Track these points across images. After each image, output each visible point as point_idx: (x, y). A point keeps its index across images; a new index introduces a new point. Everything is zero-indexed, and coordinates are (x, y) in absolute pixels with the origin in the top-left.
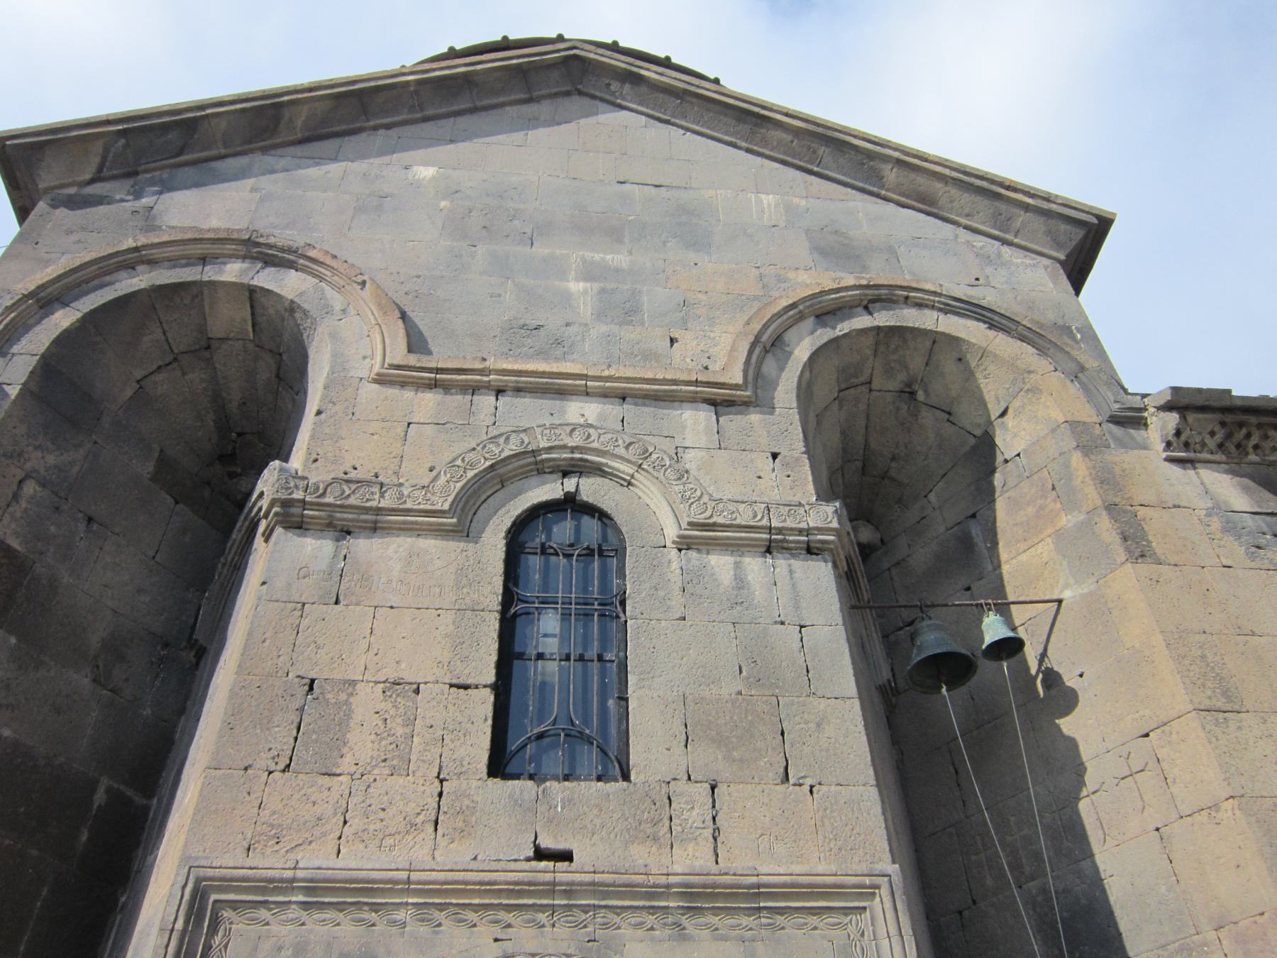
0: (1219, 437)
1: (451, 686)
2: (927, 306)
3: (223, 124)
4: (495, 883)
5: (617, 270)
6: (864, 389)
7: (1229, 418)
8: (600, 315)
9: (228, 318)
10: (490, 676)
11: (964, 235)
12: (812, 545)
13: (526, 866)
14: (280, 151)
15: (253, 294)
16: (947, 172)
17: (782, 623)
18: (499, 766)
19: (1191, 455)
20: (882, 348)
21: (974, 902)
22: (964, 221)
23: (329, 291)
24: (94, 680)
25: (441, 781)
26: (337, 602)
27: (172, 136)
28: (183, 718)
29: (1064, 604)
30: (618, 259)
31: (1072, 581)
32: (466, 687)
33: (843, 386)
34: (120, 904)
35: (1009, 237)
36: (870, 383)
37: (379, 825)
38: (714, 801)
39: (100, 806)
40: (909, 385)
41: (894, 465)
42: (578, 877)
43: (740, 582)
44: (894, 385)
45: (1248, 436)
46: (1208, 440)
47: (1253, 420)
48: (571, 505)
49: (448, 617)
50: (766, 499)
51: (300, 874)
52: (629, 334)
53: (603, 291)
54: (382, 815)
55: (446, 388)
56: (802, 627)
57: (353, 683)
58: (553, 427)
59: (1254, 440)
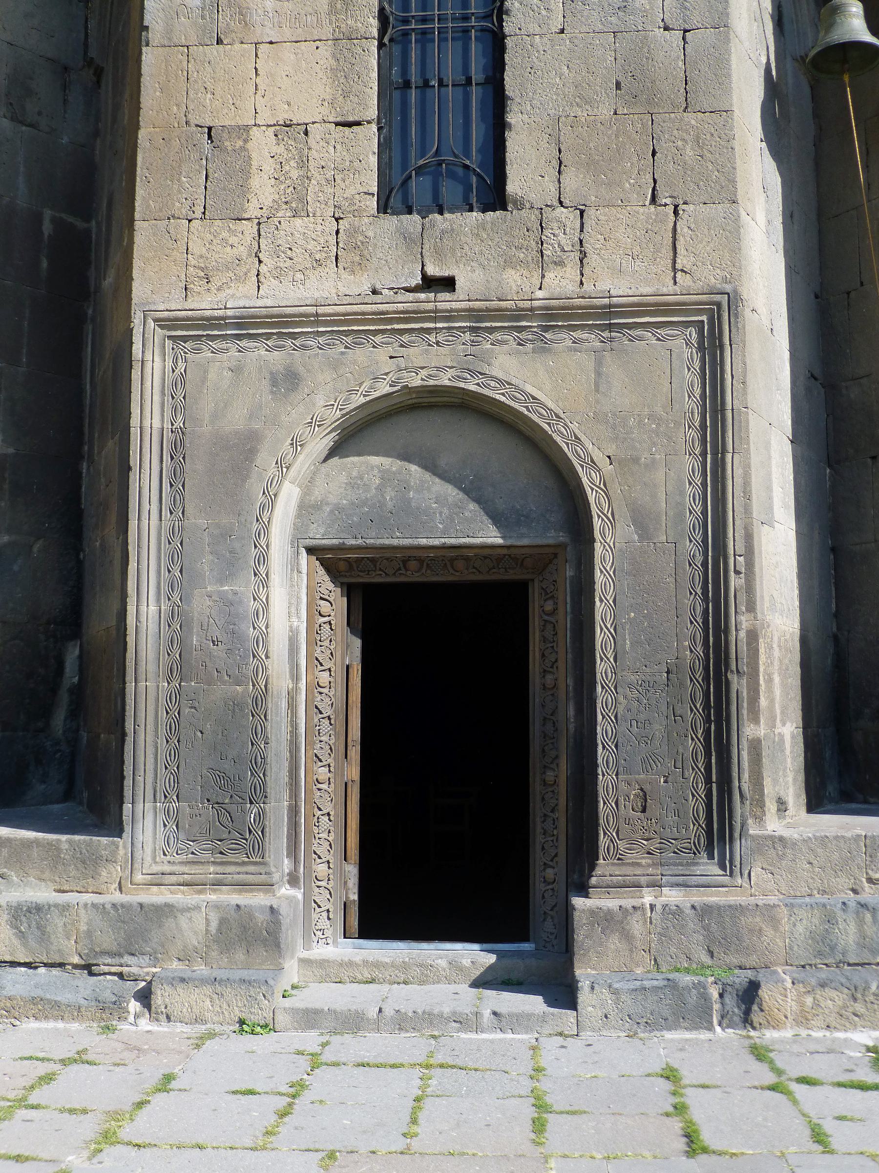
1: (337, 124)
4: (387, 313)
13: (411, 296)
17: (666, 28)
21: (862, 284)
24: (12, 119)
25: (337, 220)
26: (217, 44)
28: (98, 141)
32: (349, 125)
34: (89, 316)
37: (289, 263)
38: (582, 225)
39: (50, 236)
42: (455, 305)
49: (326, 51)
51: (230, 313)
54: (289, 252)
56: (686, 31)
57: (247, 128)
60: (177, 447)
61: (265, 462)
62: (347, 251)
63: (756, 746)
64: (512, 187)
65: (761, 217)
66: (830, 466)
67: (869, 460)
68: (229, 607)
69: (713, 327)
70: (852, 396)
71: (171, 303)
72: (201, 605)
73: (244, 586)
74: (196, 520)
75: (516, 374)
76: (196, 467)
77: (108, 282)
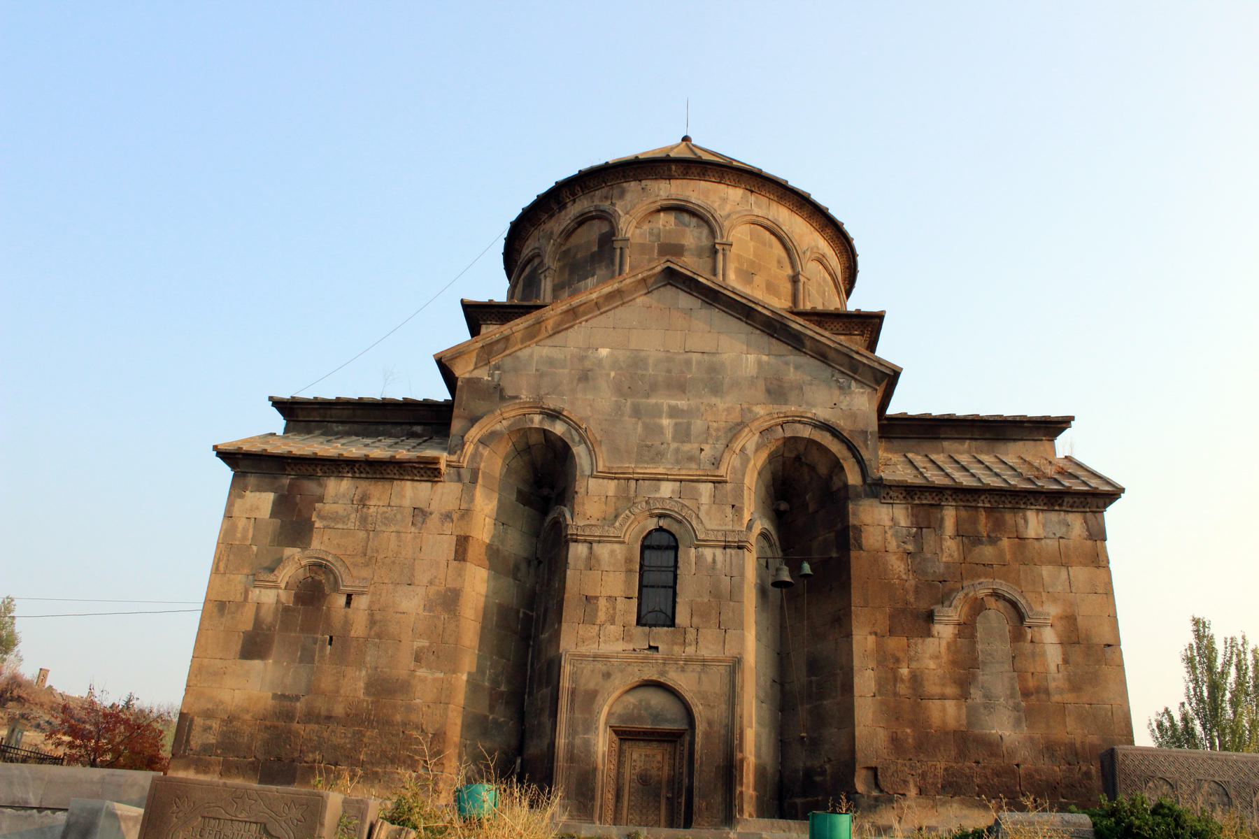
3: (519, 335)
5: (683, 411)
8: (674, 439)
9: (535, 439)
10: (636, 595)
11: (837, 375)
14: (542, 343)
15: (545, 431)
16: (832, 345)
18: (639, 622)
23: (573, 432)
27: (501, 345)
30: (682, 403)
43: (714, 561)
44: (793, 455)
48: (660, 529)
49: (623, 575)
50: (724, 528)
52: (686, 447)
53: (676, 424)
55: (619, 479)
58: (655, 499)
60: (573, 692)
61: (599, 698)
62: (626, 636)
63: (741, 793)
64: (679, 620)
65: (753, 633)
68: (587, 743)
69: (735, 665)
71: (573, 650)
72: (578, 741)
73: (590, 736)
74: (578, 715)
75: (675, 678)
76: (578, 700)
77: (545, 636)
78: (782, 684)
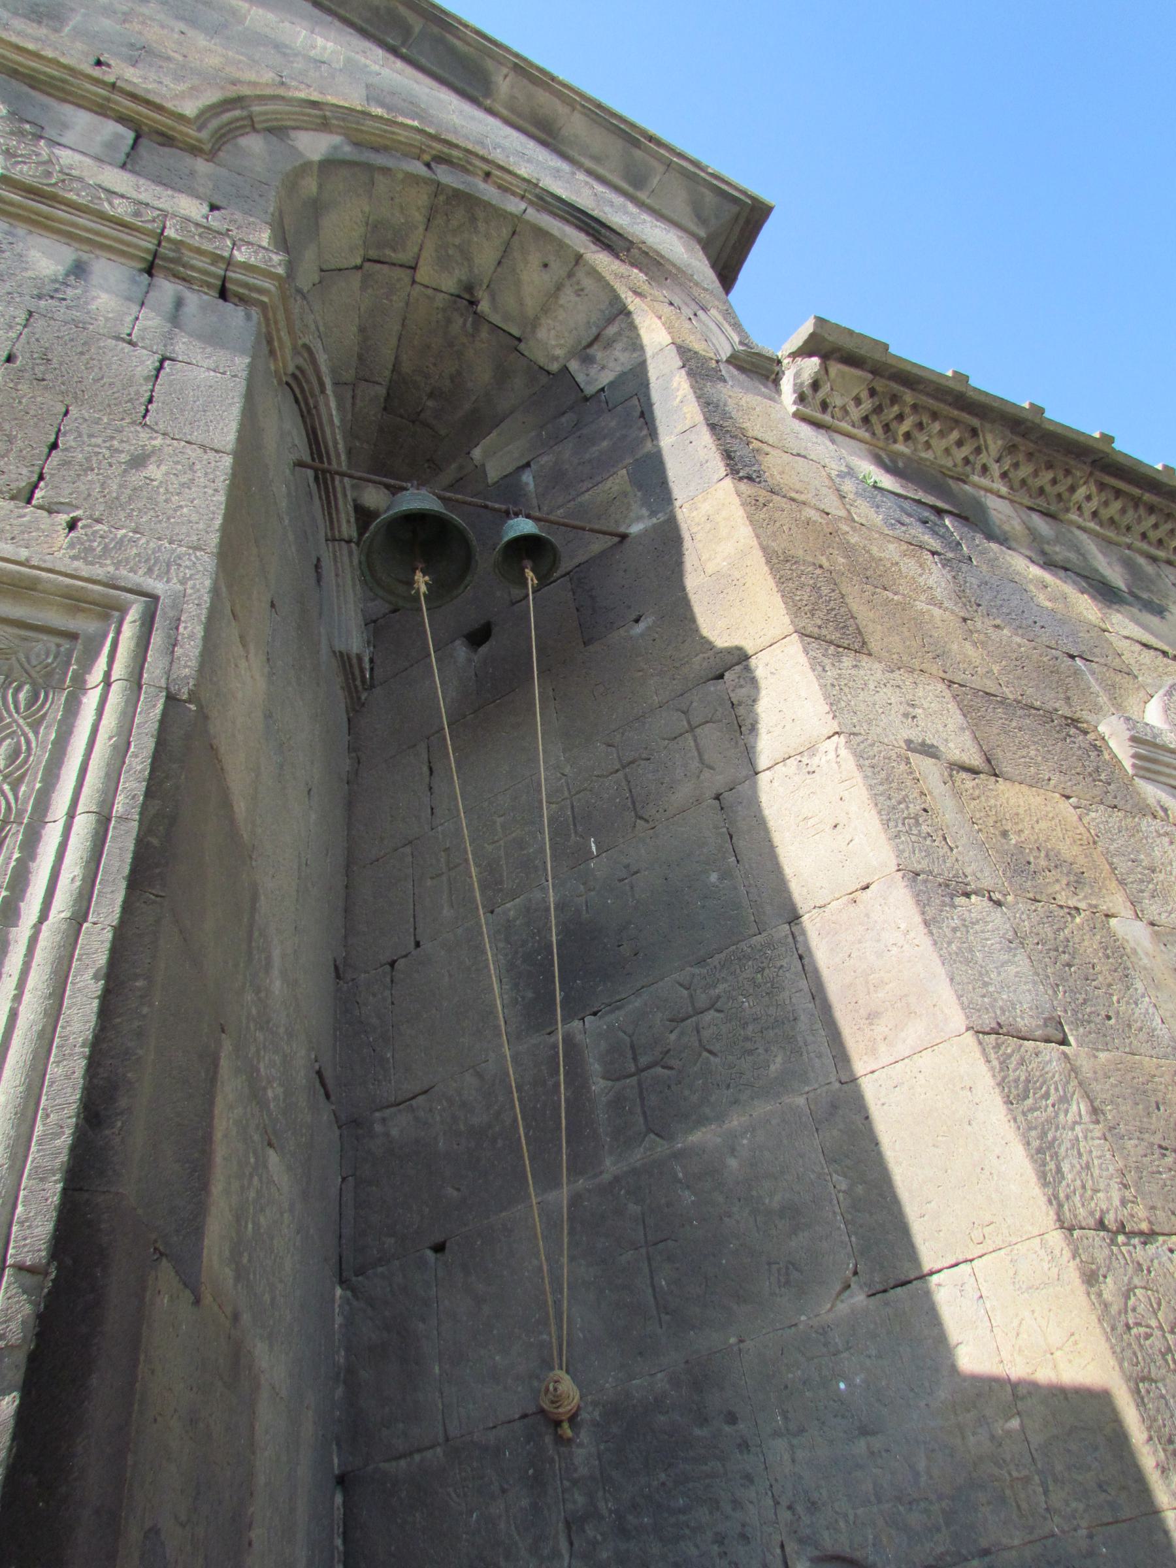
0: (867, 405)
2: (514, 194)
6: (405, 275)
7: (880, 385)
12: (229, 285)
19: (827, 418)
20: (439, 220)
21: (418, 945)
22: (588, 163)
29: (629, 540)
31: (644, 512)
33: (373, 254)
35: (642, 196)
36: (414, 268)
40: (469, 288)
41: (430, 403)
44: (449, 283)
45: (900, 418)
46: (852, 408)
47: (909, 397)
59: (905, 427)
66: (342, 1282)
67: (429, 1254)
70: (395, 1132)
78: (353, 1125)
